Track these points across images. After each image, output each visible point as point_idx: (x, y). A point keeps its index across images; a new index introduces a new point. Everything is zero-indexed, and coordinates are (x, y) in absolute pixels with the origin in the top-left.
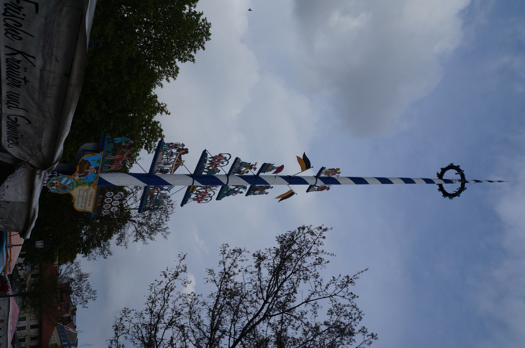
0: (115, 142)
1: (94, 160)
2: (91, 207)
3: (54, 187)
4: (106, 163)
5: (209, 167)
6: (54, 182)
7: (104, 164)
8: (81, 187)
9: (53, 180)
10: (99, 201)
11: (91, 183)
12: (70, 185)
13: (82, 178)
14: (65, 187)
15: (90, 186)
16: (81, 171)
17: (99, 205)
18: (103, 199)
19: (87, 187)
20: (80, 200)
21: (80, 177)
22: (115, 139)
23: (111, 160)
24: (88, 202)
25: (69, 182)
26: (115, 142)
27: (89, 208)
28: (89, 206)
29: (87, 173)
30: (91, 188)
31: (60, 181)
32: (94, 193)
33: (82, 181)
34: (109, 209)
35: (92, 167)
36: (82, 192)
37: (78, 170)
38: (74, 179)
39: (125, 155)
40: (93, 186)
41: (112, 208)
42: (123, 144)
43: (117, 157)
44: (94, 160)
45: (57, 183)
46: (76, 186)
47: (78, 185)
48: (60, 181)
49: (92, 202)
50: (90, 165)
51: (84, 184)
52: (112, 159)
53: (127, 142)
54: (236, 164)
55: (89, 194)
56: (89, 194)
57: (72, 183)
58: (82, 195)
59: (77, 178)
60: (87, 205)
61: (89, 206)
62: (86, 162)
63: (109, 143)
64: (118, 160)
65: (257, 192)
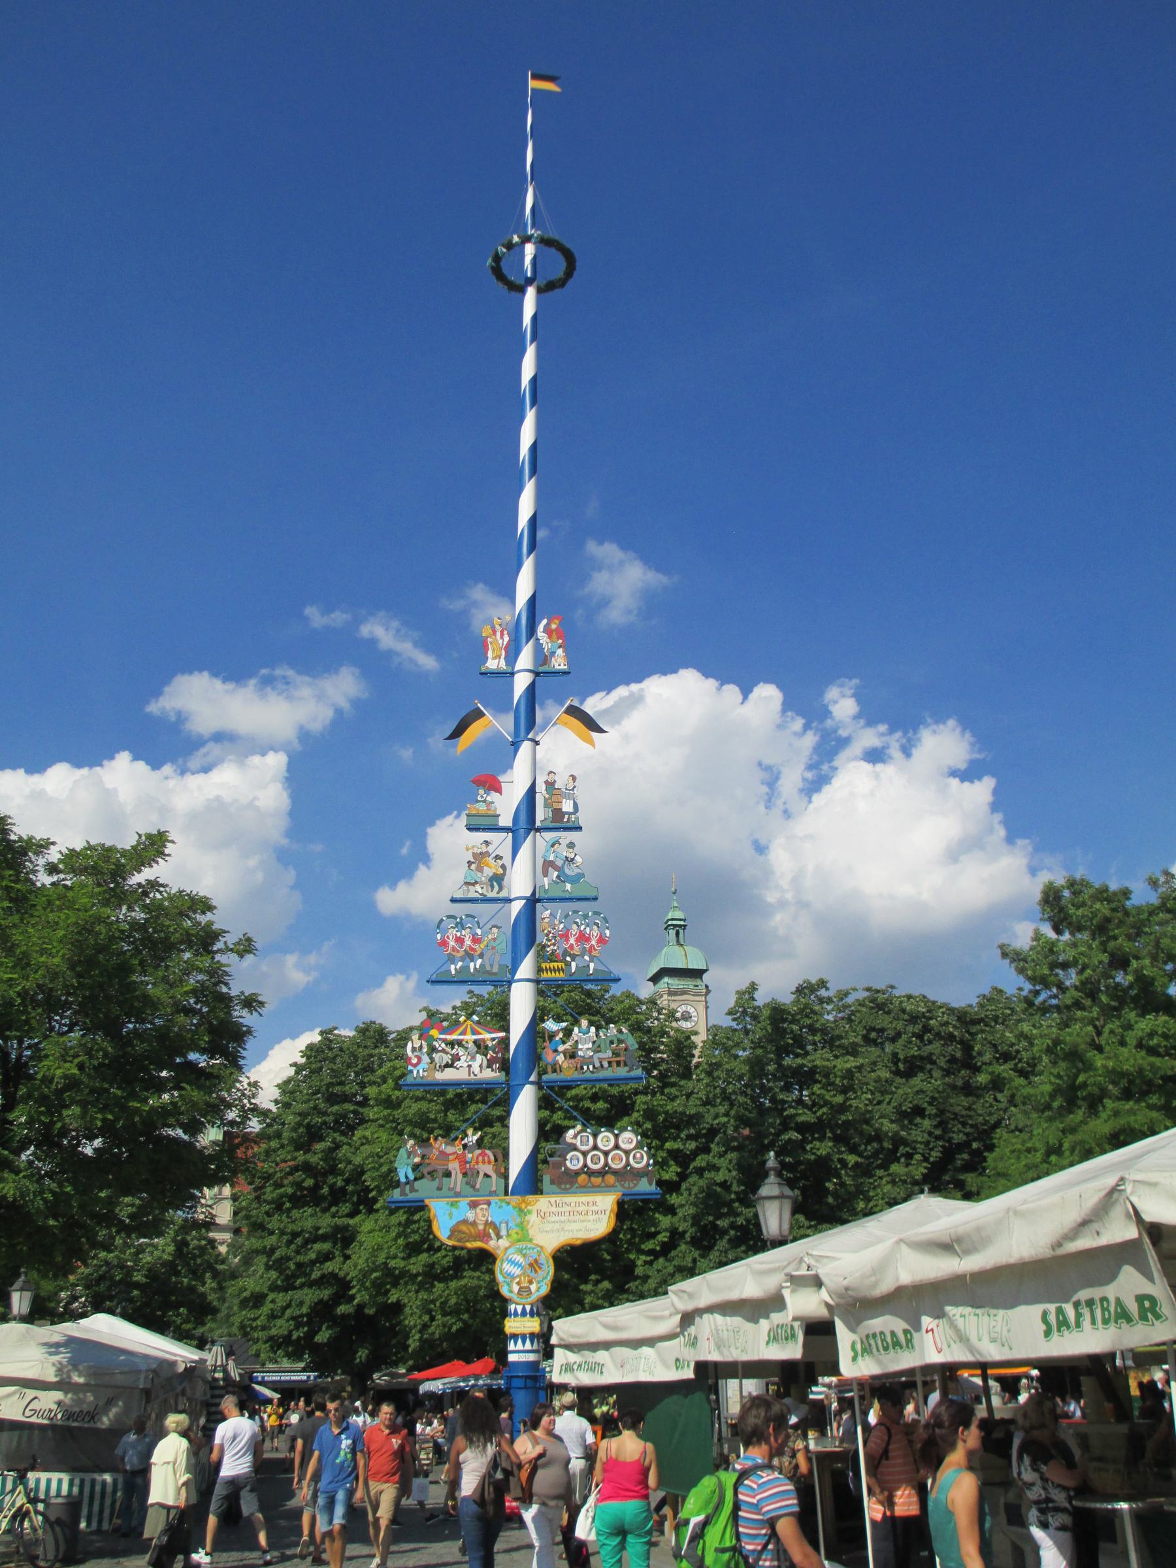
0: (411, 1176)
1: (451, 1215)
3: (533, 1287)
4: (473, 1187)
5: (481, 956)
6: (516, 1288)
7: (478, 1190)
8: (530, 1232)
9: (511, 1291)
10: (597, 1180)
11: (521, 1210)
12: (524, 1256)
13: (503, 1232)
15: (530, 1212)
16: (484, 1236)
17: (610, 1179)
18: (591, 1173)
19: (533, 1218)
20: (574, 1226)
21: (499, 1237)
22: (403, 1180)
24: (582, 1208)
25: (519, 1258)
26: (411, 1176)
27: (606, 1203)
28: (594, 1204)
29: (493, 1225)
30: (534, 1208)
32: (552, 1200)
33: (512, 1232)
34: (627, 1153)
35: (470, 1215)
36: (549, 1227)
37: (479, 1244)
38: (507, 1249)
40: (528, 1204)
41: (622, 1145)
42: (417, 1160)
43: (454, 1166)
44: (451, 1215)
45: (518, 1283)
46: (531, 1240)
47: (524, 1237)
50: (465, 1222)
51: (522, 1226)
52: (460, 1176)
53: (409, 1154)
54: (472, 895)
55: (554, 1209)
56: (554, 1209)
58: (557, 1226)
59: (503, 1243)
60: (595, 1208)
61: (594, 1204)
62: (454, 1232)
63: (413, 1190)
64: (463, 1162)
65: (567, 806)
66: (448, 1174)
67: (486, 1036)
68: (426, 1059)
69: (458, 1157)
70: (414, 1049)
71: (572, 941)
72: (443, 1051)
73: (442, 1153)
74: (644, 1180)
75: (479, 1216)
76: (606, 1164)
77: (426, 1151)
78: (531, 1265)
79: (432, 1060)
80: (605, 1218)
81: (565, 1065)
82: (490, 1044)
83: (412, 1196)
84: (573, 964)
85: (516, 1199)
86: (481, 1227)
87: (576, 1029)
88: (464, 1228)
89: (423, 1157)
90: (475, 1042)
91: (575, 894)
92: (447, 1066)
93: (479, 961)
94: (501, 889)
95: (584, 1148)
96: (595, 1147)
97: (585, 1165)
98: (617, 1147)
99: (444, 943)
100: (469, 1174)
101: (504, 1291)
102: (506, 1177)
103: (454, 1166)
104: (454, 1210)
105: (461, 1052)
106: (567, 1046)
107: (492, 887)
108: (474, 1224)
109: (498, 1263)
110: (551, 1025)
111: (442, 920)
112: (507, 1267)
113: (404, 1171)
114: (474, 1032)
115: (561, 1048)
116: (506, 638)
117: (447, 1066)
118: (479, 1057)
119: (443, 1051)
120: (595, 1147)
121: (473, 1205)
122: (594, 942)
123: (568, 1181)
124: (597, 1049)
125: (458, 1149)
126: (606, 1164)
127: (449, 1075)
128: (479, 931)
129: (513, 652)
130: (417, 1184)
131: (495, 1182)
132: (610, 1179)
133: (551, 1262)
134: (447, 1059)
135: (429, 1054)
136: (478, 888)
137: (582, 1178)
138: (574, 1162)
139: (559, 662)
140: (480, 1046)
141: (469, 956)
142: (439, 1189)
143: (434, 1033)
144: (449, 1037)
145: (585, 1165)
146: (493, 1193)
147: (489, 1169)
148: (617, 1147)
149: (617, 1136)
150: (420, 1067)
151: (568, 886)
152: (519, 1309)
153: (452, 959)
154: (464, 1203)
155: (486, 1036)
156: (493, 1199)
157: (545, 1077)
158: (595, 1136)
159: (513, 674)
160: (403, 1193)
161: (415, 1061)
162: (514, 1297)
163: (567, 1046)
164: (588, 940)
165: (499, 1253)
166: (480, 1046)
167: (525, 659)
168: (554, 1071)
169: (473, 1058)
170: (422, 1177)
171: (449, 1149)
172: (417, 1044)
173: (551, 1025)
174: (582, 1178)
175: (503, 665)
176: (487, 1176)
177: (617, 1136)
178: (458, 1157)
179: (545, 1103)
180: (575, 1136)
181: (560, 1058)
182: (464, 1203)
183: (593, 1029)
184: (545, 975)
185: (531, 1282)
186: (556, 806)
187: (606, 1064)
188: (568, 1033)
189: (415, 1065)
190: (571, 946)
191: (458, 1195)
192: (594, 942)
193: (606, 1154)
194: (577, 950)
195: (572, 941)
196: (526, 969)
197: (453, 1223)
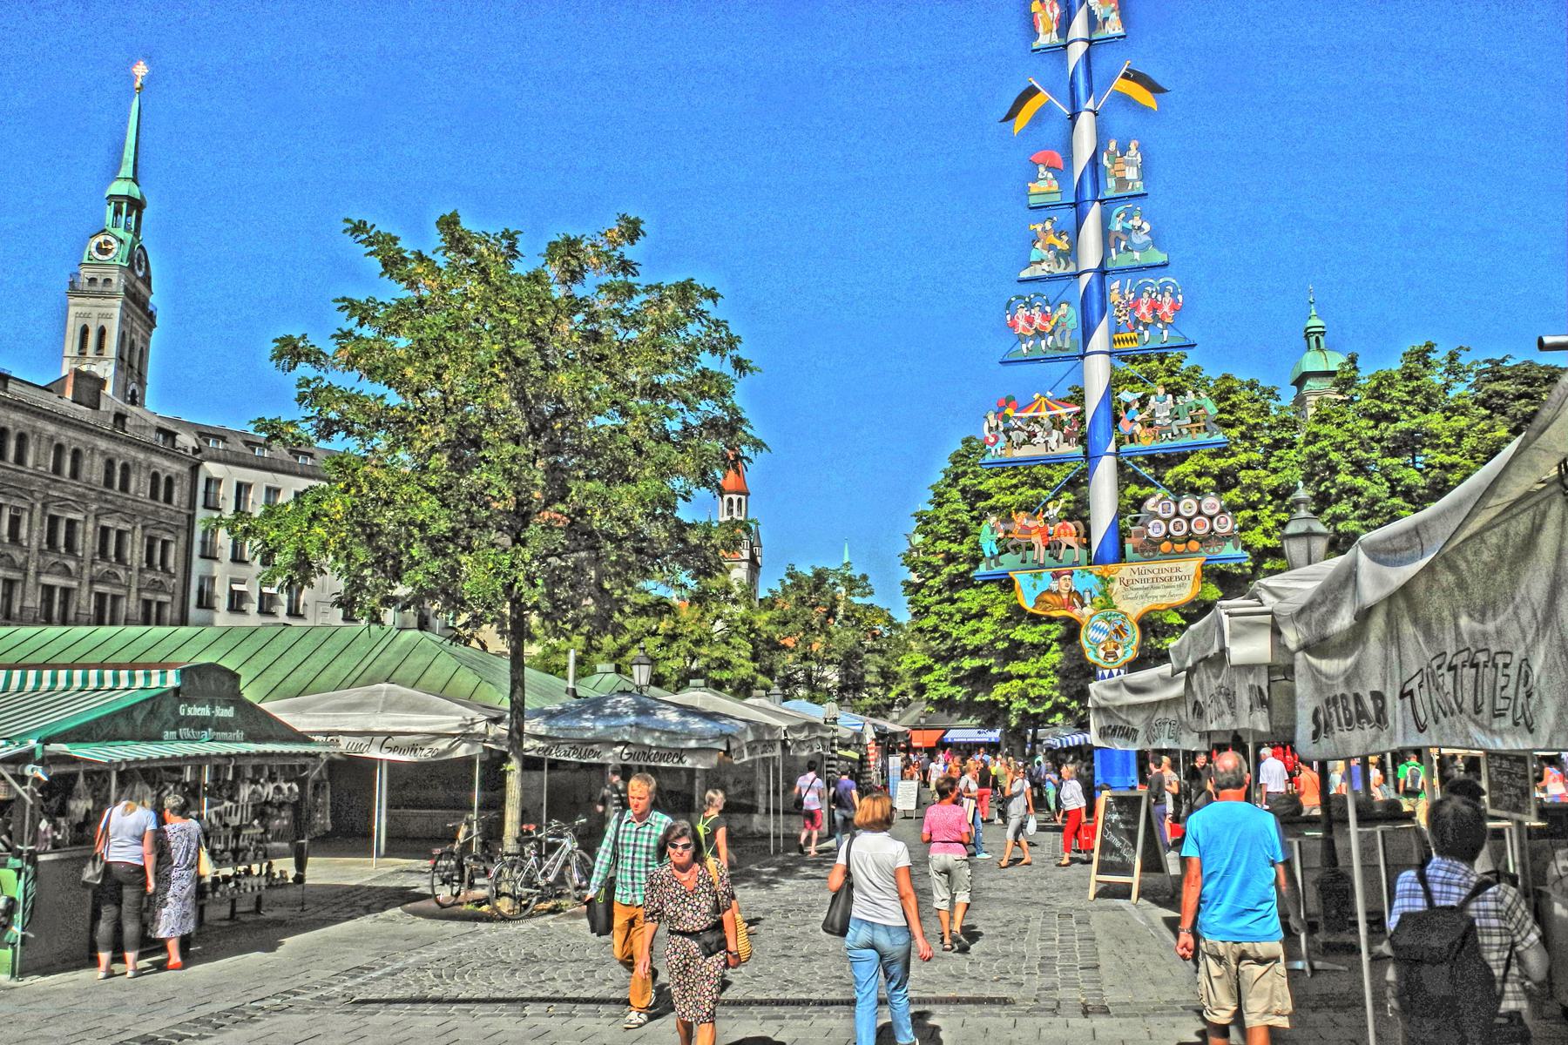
1: (1034, 586)
2: (1181, 564)
3: (1119, 652)
6: (1102, 654)
10: (1180, 547)
11: (1104, 579)
13: (1087, 600)
14: (1116, 631)
15: (1113, 580)
17: (1194, 545)
19: (1116, 586)
20: (1158, 592)
21: (1083, 605)
22: (988, 555)
23: (1048, 548)
25: (1104, 625)
28: (1178, 570)
30: (1117, 576)
31: (1099, 644)
34: (1211, 518)
35: (1054, 586)
39: (1031, 524)
42: (1001, 535)
43: (1036, 539)
44: (1034, 586)
47: (1109, 604)
48: (1099, 644)
49: (1166, 566)
50: (1049, 591)
51: (1105, 594)
53: (993, 530)
57: (1105, 618)
59: (1088, 610)
61: (1178, 570)
66: (1031, 548)
67: (1061, 411)
68: (1003, 437)
69: (1040, 530)
70: (990, 429)
71: (1144, 309)
72: (1020, 429)
73: (1024, 527)
74: (1229, 545)
75: (1062, 585)
76: (1190, 530)
77: (1009, 526)
78: (1116, 631)
79: (1009, 438)
80: (1189, 583)
81: (1143, 435)
82: (1065, 419)
83: (997, 570)
84: (1147, 333)
85: (1097, 569)
86: (1065, 597)
87: (1153, 398)
88: (1048, 598)
89: (1007, 532)
90: (1053, 419)
91: (1144, 262)
92: (1024, 442)
93: (1050, 338)
94: (1067, 264)
95: (1166, 516)
96: (1177, 514)
97: (1168, 533)
98: (1200, 513)
99: (1014, 325)
100: (1052, 547)
101: (1091, 656)
102: (1088, 546)
103: (1036, 539)
104: (1039, 583)
105: (1037, 428)
106: (1144, 415)
107: (1059, 263)
108: (1058, 593)
109: (1083, 630)
110: (1126, 396)
111: (1010, 302)
112: (1092, 634)
113: (988, 546)
114: (1049, 408)
115: (1138, 418)
116: (1057, 11)
117: (1024, 442)
118: (1055, 433)
119: (1020, 429)
120: (1177, 514)
121: (1056, 576)
122: (1166, 309)
123: (1151, 549)
124: (1176, 416)
125: (1040, 522)
126: (1190, 530)
127: (1026, 452)
128: (1048, 309)
129: (1065, 24)
130: (1002, 559)
131: (1079, 553)
132: (1194, 545)
133: (1136, 628)
134: (1023, 436)
135: (1006, 432)
136: (1044, 265)
137: (1165, 546)
138: (1156, 530)
139: (1114, 28)
140: (1057, 423)
141: (1040, 334)
142: (1024, 561)
143: (1009, 411)
144: (1024, 415)
145: (1168, 533)
146: (1076, 564)
147: (1071, 541)
148: (1200, 513)
149: (1199, 502)
150: (998, 446)
151: (1137, 255)
152: (1106, 673)
153: (1022, 339)
154: (1047, 574)
155: (1061, 411)
156: (1076, 570)
157: (1122, 448)
158: (1177, 503)
159: (1066, 46)
160: (989, 567)
161: (992, 440)
162: (1101, 663)
163: (1144, 415)
164: (1161, 306)
165: (1085, 620)
166: (1057, 423)
167: (1079, 27)
168: (1132, 441)
169: (1050, 434)
170: (1007, 551)
171: (1031, 524)
172: (993, 424)
173: (1126, 396)
174: (1165, 546)
175: (1055, 39)
176: (1068, 547)
177: (1199, 502)
178: (1040, 530)
179: (1125, 475)
180: (1156, 505)
181: (1138, 428)
182: (1047, 574)
183: (1170, 397)
184: (1117, 347)
185: (1116, 648)
186: (1119, 175)
187: (1185, 431)
188: (1143, 402)
189: (993, 444)
190: (1143, 315)
191: (1042, 566)
192: (1166, 309)
193: (1189, 520)
194: (1149, 319)
195: (1144, 309)
196: (1099, 340)
197: (1037, 593)
